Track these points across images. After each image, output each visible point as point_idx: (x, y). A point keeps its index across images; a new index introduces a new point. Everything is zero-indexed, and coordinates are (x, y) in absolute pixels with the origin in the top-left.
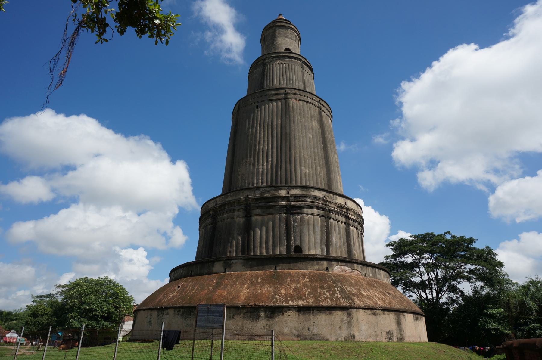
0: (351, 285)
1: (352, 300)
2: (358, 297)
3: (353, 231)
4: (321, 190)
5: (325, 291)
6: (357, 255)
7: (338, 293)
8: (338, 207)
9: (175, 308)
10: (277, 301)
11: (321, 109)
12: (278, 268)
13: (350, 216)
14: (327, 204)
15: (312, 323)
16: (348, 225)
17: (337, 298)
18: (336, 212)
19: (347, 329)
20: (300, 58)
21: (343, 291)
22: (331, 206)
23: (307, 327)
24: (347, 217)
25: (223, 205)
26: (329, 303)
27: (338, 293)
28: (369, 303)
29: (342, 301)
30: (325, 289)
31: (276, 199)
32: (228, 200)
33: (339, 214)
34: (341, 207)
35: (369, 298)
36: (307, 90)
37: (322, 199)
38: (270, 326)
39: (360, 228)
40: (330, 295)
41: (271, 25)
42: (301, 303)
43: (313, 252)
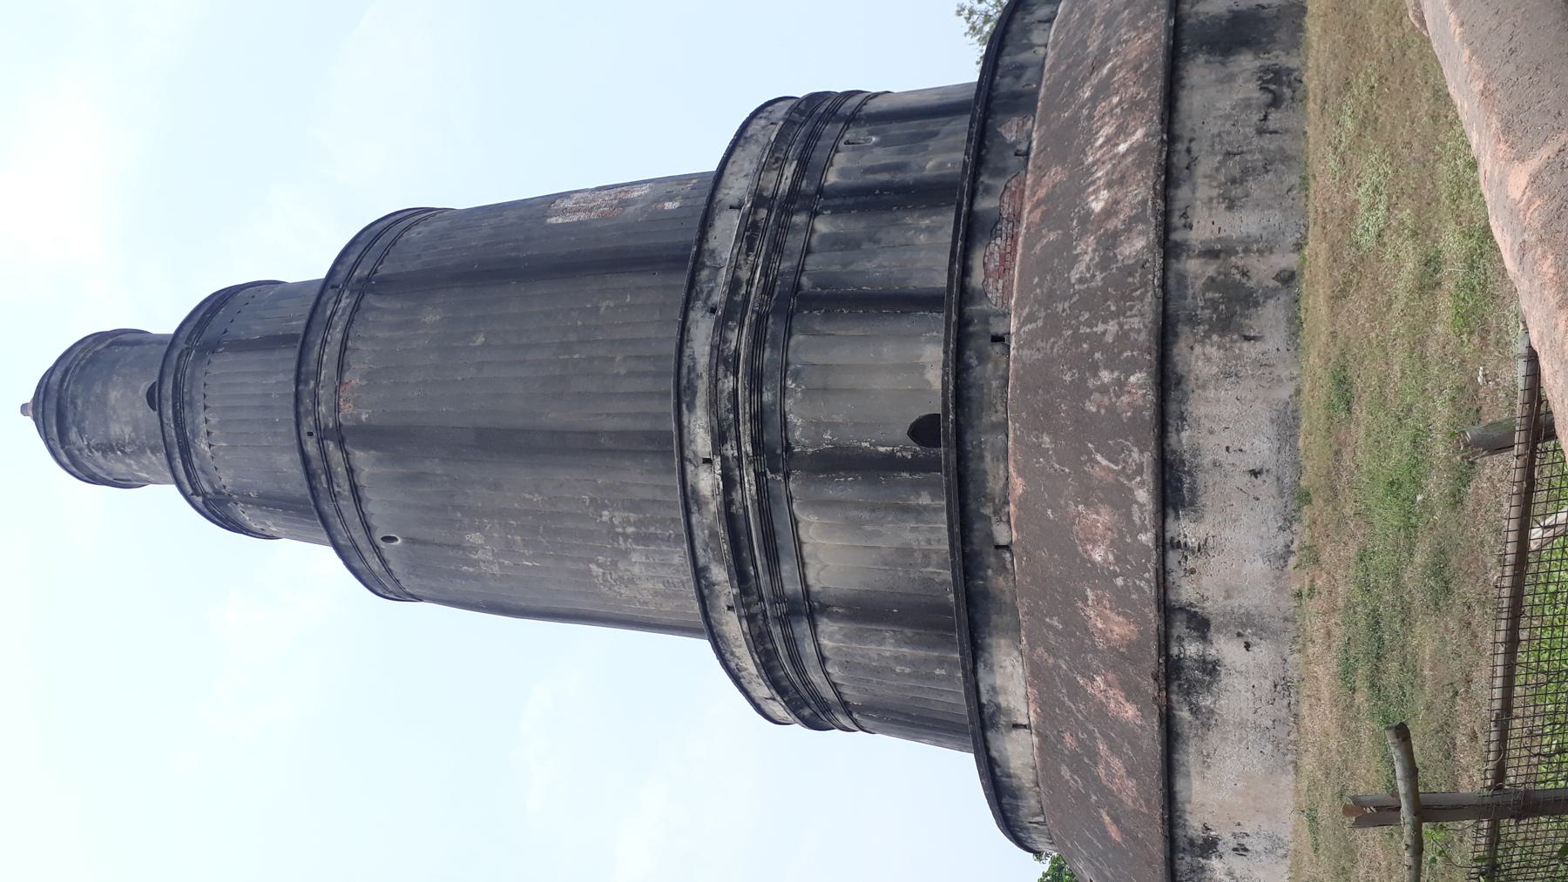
0: (1065, 250)
1: (1128, 271)
3: (843, 172)
4: (684, 329)
5: (1091, 383)
6: (943, 157)
7: (1100, 328)
10: (1139, 590)
11: (368, 279)
12: (1002, 540)
13: (785, 186)
14: (738, 298)
17: (1123, 336)
18: (768, 258)
19: (1256, 304)
20: (170, 371)
21: (1091, 302)
23: (1247, 477)
24: (794, 199)
25: (774, 683)
27: (1100, 328)
28: (1140, 191)
29: (1136, 323)
30: (1083, 380)
32: (753, 670)
33: (777, 248)
34: (749, 233)
35: (1117, 182)
36: (298, 325)
37: (721, 326)
38: (1244, 625)
39: (830, 130)
41: (65, 460)
42: (1143, 495)
43: (934, 377)
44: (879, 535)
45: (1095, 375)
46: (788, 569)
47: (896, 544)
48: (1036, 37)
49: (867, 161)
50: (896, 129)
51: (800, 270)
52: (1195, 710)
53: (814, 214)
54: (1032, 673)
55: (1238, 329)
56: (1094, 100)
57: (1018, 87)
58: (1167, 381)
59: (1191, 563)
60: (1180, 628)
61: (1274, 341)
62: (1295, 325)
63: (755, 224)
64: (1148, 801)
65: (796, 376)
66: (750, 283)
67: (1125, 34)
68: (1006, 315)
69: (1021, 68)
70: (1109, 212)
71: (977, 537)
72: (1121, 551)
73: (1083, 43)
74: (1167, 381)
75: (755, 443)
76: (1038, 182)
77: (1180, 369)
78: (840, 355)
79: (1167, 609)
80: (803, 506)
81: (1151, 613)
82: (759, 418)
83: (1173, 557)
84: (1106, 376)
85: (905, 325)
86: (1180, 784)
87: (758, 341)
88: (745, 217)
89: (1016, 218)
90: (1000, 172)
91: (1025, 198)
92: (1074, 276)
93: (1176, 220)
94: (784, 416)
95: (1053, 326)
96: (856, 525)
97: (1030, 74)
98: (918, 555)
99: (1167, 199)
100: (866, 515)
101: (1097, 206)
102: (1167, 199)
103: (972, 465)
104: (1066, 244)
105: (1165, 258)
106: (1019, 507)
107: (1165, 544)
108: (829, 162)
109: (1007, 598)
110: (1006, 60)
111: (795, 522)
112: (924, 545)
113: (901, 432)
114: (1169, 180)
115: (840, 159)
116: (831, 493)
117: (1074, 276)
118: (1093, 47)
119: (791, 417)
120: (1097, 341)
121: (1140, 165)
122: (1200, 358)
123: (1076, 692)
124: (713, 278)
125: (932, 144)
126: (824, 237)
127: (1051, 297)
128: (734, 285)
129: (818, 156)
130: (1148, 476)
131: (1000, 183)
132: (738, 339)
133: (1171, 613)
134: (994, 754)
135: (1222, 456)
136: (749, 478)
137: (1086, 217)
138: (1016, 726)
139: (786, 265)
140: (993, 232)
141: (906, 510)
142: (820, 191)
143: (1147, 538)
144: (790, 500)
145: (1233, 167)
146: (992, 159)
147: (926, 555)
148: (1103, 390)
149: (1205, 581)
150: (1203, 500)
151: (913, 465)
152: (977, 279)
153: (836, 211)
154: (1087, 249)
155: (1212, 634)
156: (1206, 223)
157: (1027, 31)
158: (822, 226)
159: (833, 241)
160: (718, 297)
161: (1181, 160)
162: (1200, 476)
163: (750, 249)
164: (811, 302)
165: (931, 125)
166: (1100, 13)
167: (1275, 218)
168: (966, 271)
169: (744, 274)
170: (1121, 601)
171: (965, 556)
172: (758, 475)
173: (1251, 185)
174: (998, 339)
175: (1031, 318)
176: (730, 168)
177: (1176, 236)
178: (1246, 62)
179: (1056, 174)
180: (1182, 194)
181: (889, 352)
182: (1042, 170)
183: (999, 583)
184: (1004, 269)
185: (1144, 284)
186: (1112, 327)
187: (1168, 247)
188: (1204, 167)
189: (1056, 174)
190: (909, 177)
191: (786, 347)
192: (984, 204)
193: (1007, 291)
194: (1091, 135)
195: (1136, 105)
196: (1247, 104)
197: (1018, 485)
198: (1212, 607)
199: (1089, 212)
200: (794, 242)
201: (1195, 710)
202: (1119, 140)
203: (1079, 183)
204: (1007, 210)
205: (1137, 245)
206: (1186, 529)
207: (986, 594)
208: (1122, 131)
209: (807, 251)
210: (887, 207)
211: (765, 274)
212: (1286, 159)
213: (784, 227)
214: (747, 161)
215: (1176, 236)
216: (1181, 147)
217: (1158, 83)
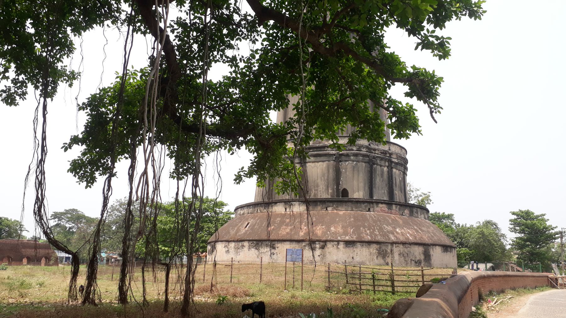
3: (395, 172)
5: (366, 229)
9: (249, 241)
12: (328, 209)
13: (394, 160)
16: (390, 168)
17: (376, 235)
18: (380, 157)
21: (381, 229)
22: (375, 153)
26: (369, 238)
28: (402, 239)
29: (379, 237)
31: (326, 149)
33: (382, 159)
34: (384, 152)
37: (367, 147)
42: (347, 238)
44: (321, 180)
46: (312, 159)
47: (319, 184)
48: (422, 216)
49: (397, 177)
50: (402, 184)
51: (377, 164)
52: (305, 246)
56: (415, 229)
58: (369, 243)
60: (322, 244)
61: (376, 261)
62: (380, 265)
63: (386, 154)
65: (356, 164)
66: (375, 153)
67: (427, 235)
70: (397, 232)
73: (424, 226)
74: (369, 243)
75: (342, 154)
76: (398, 218)
77: (372, 245)
78: (361, 175)
79: (325, 242)
80: (327, 164)
81: (324, 239)
82: (347, 155)
83: (336, 243)
84: (368, 232)
85: (367, 188)
86: (288, 243)
87: (364, 156)
89: (391, 214)
90: (399, 209)
91: (394, 215)
93: (397, 245)
95: (375, 222)
96: (323, 175)
98: (316, 188)
100: (326, 178)
101: (397, 230)
103: (344, 204)
104: (390, 224)
107: (338, 241)
108: (397, 169)
109: (316, 209)
110: (419, 210)
111: (323, 161)
112: (319, 190)
113: (344, 187)
114: (404, 244)
116: (331, 171)
118: (423, 228)
119: (347, 163)
120: (374, 230)
121: (406, 238)
122: (374, 249)
123: (301, 223)
126: (383, 169)
127: (380, 221)
128: (375, 150)
129: (399, 167)
130: (351, 239)
131: (397, 210)
132: (364, 151)
133: (324, 243)
135: (356, 252)
136: (334, 152)
137: (395, 228)
138: (286, 209)
139: (378, 161)
140: (389, 209)
141: (328, 187)
142: (392, 168)
143: (339, 238)
144: (329, 161)
145: (406, 255)
146: (402, 208)
147: (317, 190)
148: (366, 231)
149: (332, 249)
150: (347, 249)
151: (338, 189)
152: (380, 205)
153: (388, 172)
154: (390, 228)
155: (321, 250)
156: (397, 250)
157: (423, 213)
158: (385, 169)
159: (382, 172)
161: (407, 246)
162: (352, 248)
164: (371, 167)
165: (403, 191)
166: (429, 230)
167: (397, 262)
168: (382, 203)
169: (377, 152)
170: (324, 233)
172: (334, 155)
173: (403, 258)
174: (369, 210)
175: (375, 217)
177: (394, 245)
178: (422, 257)
179: (401, 222)
180: (401, 246)
181: (361, 185)
182: (400, 218)
183: (319, 208)
184: (382, 211)
186: (377, 233)
187: (393, 243)
188: (406, 250)
189: (401, 222)
190: (394, 188)
191: (362, 162)
192: (394, 206)
194: (409, 229)
195: (415, 237)
196: (416, 257)
197: (341, 213)
200: (383, 163)
201: (305, 246)
202: (408, 234)
205: (393, 238)
206: (341, 246)
207: (316, 205)
208: (411, 235)
209: (381, 166)
210: (389, 183)
211: (377, 157)
212: (407, 264)
213: (386, 160)
214: (397, 150)
215: (394, 245)
217: (419, 242)
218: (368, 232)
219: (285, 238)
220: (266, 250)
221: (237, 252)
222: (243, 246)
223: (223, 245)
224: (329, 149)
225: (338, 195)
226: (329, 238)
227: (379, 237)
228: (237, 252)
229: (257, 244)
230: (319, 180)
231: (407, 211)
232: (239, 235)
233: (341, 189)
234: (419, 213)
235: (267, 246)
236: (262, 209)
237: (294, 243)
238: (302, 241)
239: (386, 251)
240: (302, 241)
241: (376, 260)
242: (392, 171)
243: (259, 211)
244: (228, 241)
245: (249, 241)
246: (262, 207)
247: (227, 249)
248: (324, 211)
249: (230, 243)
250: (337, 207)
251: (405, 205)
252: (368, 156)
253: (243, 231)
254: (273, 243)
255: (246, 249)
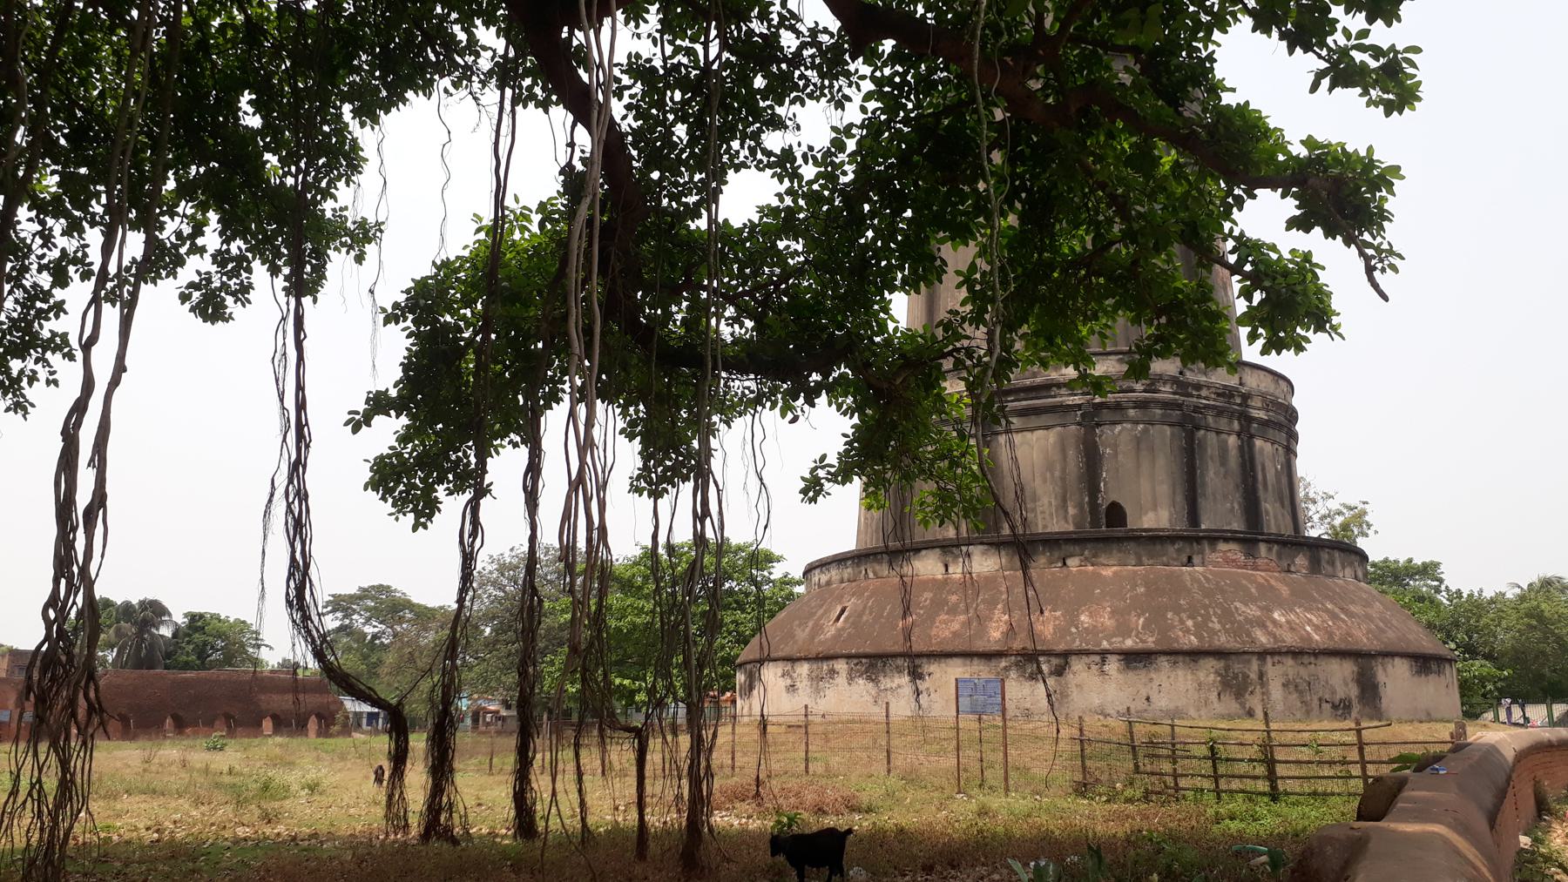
0: (1248, 599)
1: (1249, 635)
2: (1263, 626)
3: (1262, 449)
5: (1184, 616)
8: (1219, 395)
12: (1069, 562)
13: (1255, 413)
15: (1155, 685)
16: (1246, 436)
17: (1214, 632)
18: (1214, 407)
21: (1227, 615)
24: (1247, 419)
26: (1192, 641)
28: (1290, 639)
29: (1223, 639)
33: (1220, 412)
34: (1227, 393)
35: (1292, 627)
37: (1174, 380)
40: (1195, 625)
42: (1129, 643)
44: (1045, 481)
45: (1189, 617)
47: (1039, 492)
48: (1348, 571)
49: (1268, 464)
50: (1284, 480)
51: (1207, 429)
53: (1239, 435)
54: (986, 578)
55: (1224, 690)
56: (1327, 611)
57: (1324, 564)
58: (1194, 655)
59: (1094, 667)
60: (1055, 661)
61: (1219, 707)
62: (1230, 717)
64: (940, 643)
65: (1145, 431)
66: (1199, 397)
67: (1363, 627)
68: (1203, 564)
69: (1332, 563)
70: (1275, 622)
71: (1071, 548)
72: (1093, 631)
73: (1353, 602)
74: (1194, 655)
76: (1277, 579)
77: (1202, 662)
78: (1161, 461)
79: (1066, 655)
81: (1062, 647)
82: (1118, 407)
83: (1097, 658)
84: (1190, 623)
85: (1179, 498)
87: (1166, 405)
88: (1236, 390)
89: (1255, 568)
90: (1279, 556)
91: (1265, 573)
92: (1238, 605)
93: (1277, 658)
94: (1120, 423)
95: (1208, 593)
96: (1050, 467)
97: (1330, 569)
99: (1287, 653)
100: (1057, 474)
101: (1276, 615)
102: (1287, 653)
103: (1115, 546)
104: (1253, 600)
105: (1259, 653)
106: (1093, 573)
107: (1104, 654)
108: (1266, 440)
110: (1337, 554)
111: (1047, 428)
113: (1114, 497)
114: (1296, 654)
115: (1268, 447)
116: (1071, 453)
117: (1238, 605)
118: (1352, 608)
119: (1118, 428)
120: (1207, 618)
121: (1302, 638)
122: (1208, 671)
123: (992, 604)
124: (1200, 371)
125: (1278, 505)
127: (1223, 592)
128: (1198, 387)
129: (1271, 433)
130: (1141, 646)
131: (1274, 557)
132: (1166, 392)
134: (924, 552)
136: (1077, 400)
138: (946, 567)
139: (1210, 419)
140: (1249, 554)
141: (1064, 500)
142: (1252, 437)
143: (1105, 645)
144: (1064, 426)
146: (1286, 550)
148: (1182, 622)
149: (1085, 675)
152: (1222, 546)
153: (1241, 448)
154: (1253, 611)
156: (1276, 673)
157: (1351, 565)
158: (1232, 441)
159: (1224, 449)
160: (1190, 376)
161: (1306, 659)
163: (1219, 395)
164: (1190, 438)
165: (1287, 503)
167: (1280, 707)
168: (1226, 540)
169: (1204, 393)
170: (1062, 632)
171: (1057, 540)
172: (1079, 406)
173: (1295, 695)
174: (1190, 559)
175: (1207, 579)
176: (1262, 373)
177: (1269, 658)
178: (1354, 691)
179: (1285, 591)
180: (1289, 661)
181: (1164, 489)
182: (1283, 581)
184: (1227, 561)
185: (1244, 643)
186: (1217, 626)
187: (1263, 654)
188: (1303, 672)
189: (1285, 591)
190: (1261, 493)
191: (1163, 423)
192: (1263, 548)
193: (1216, 564)
194: (1309, 610)
195: (1331, 635)
196: (1334, 692)
197: (1107, 572)
198: (1070, 678)
199: (1272, 611)
200: (1223, 423)
203: (1287, 607)
204: (1259, 561)
205: (1263, 639)
206: (1113, 665)
208: (1317, 628)
209: (1218, 432)
210: (1244, 481)
211: (1207, 407)
212: (1308, 713)
215: (1269, 658)
216: (1312, 659)
217: (1343, 646)
218: (1190, 623)
219: (949, 648)
220: (897, 681)
221: (818, 690)
222: (833, 673)
223: (779, 672)
224: (1063, 391)
225: (1095, 523)
226: (1076, 645)
227: (1223, 639)
228: (818, 690)
229: (872, 666)
230: (1038, 481)
231: (1301, 561)
232: (820, 642)
233: (1106, 498)
234: (1338, 564)
235: (899, 670)
236: (877, 567)
237: (976, 661)
238: (999, 655)
239: (1246, 677)
240: (999, 655)
241: (1216, 705)
242: (1251, 446)
243: (871, 575)
244: (792, 660)
245: (849, 657)
246: (880, 562)
247: (789, 682)
248: (1056, 569)
249: (797, 664)
250: (1095, 556)
251: (1295, 543)
252: (1179, 406)
253: (830, 630)
254: (917, 662)
255: (841, 680)
